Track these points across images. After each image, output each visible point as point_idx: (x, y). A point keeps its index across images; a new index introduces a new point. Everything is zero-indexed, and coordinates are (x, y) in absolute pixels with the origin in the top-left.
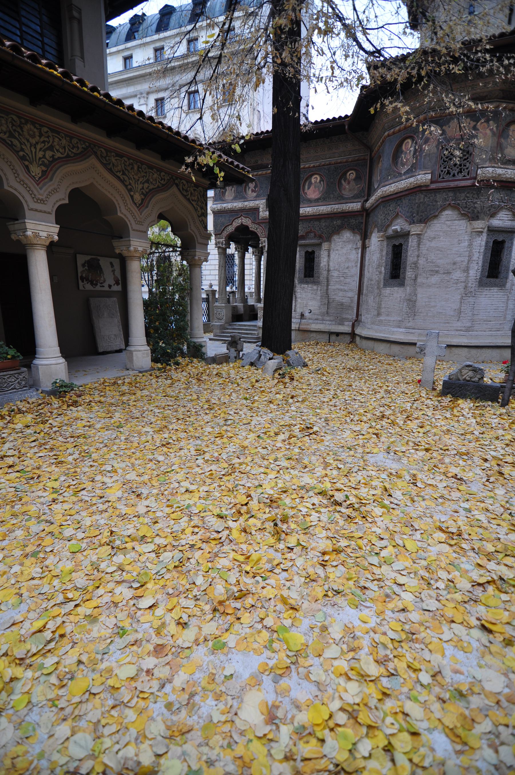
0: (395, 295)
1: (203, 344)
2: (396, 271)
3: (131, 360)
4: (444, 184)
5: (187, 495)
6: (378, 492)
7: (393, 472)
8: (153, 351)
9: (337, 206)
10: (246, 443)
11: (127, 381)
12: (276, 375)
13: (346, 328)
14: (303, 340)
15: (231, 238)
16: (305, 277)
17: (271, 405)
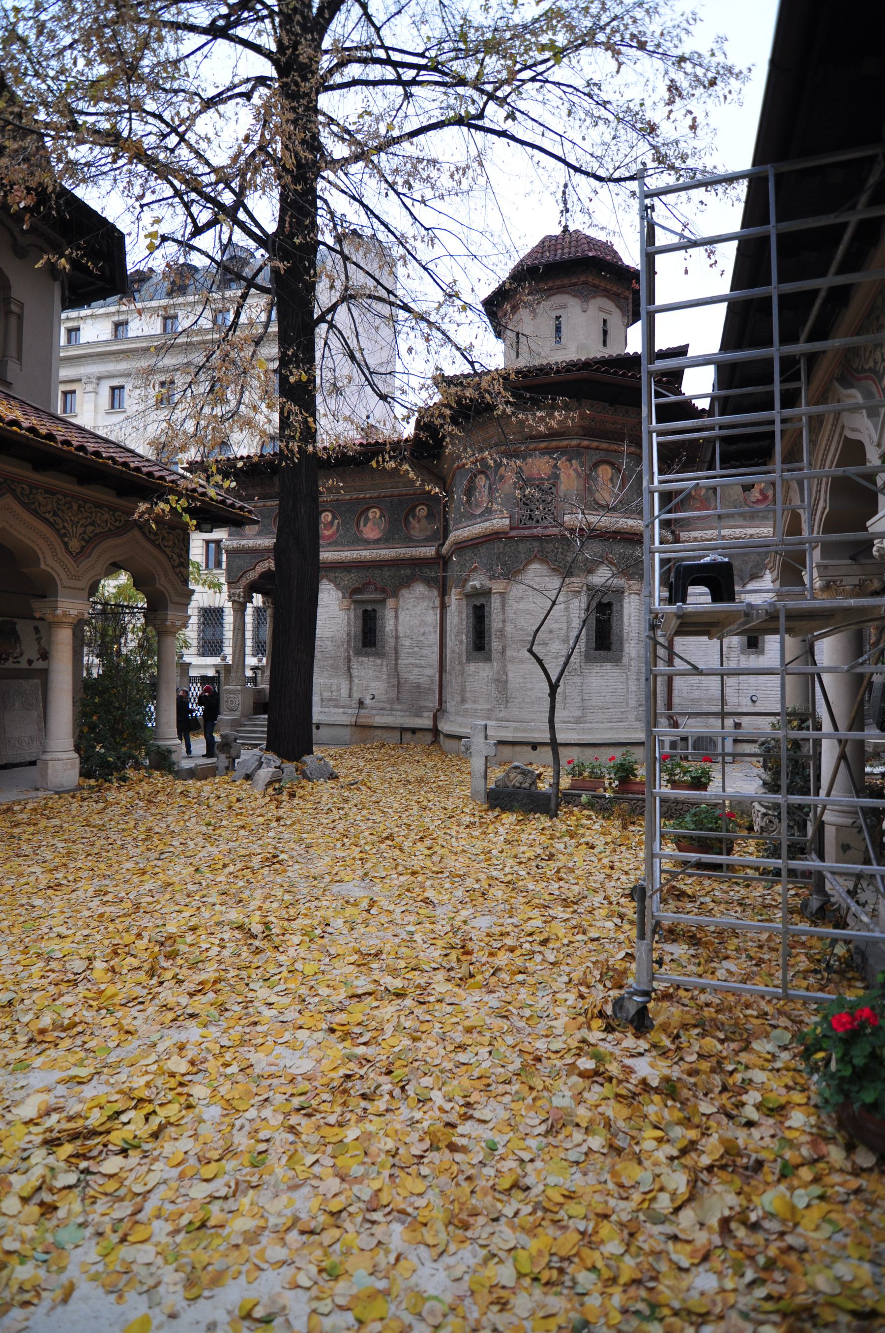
0: (480, 674)
1: (173, 748)
2: (480, 641)
3: (44, 775)
4: (526, 532)
5: (57, 940)
6: (315, 923)
7: (352, 900)
8: (84, 760)
9: (403, 551)
10: (175, 879)
11: (30, 806)
12: (270, 791)
13: (426, 722)
14: (364, 741)
15: (253, 588)
16: (364, 645)
17: (242, 832)
